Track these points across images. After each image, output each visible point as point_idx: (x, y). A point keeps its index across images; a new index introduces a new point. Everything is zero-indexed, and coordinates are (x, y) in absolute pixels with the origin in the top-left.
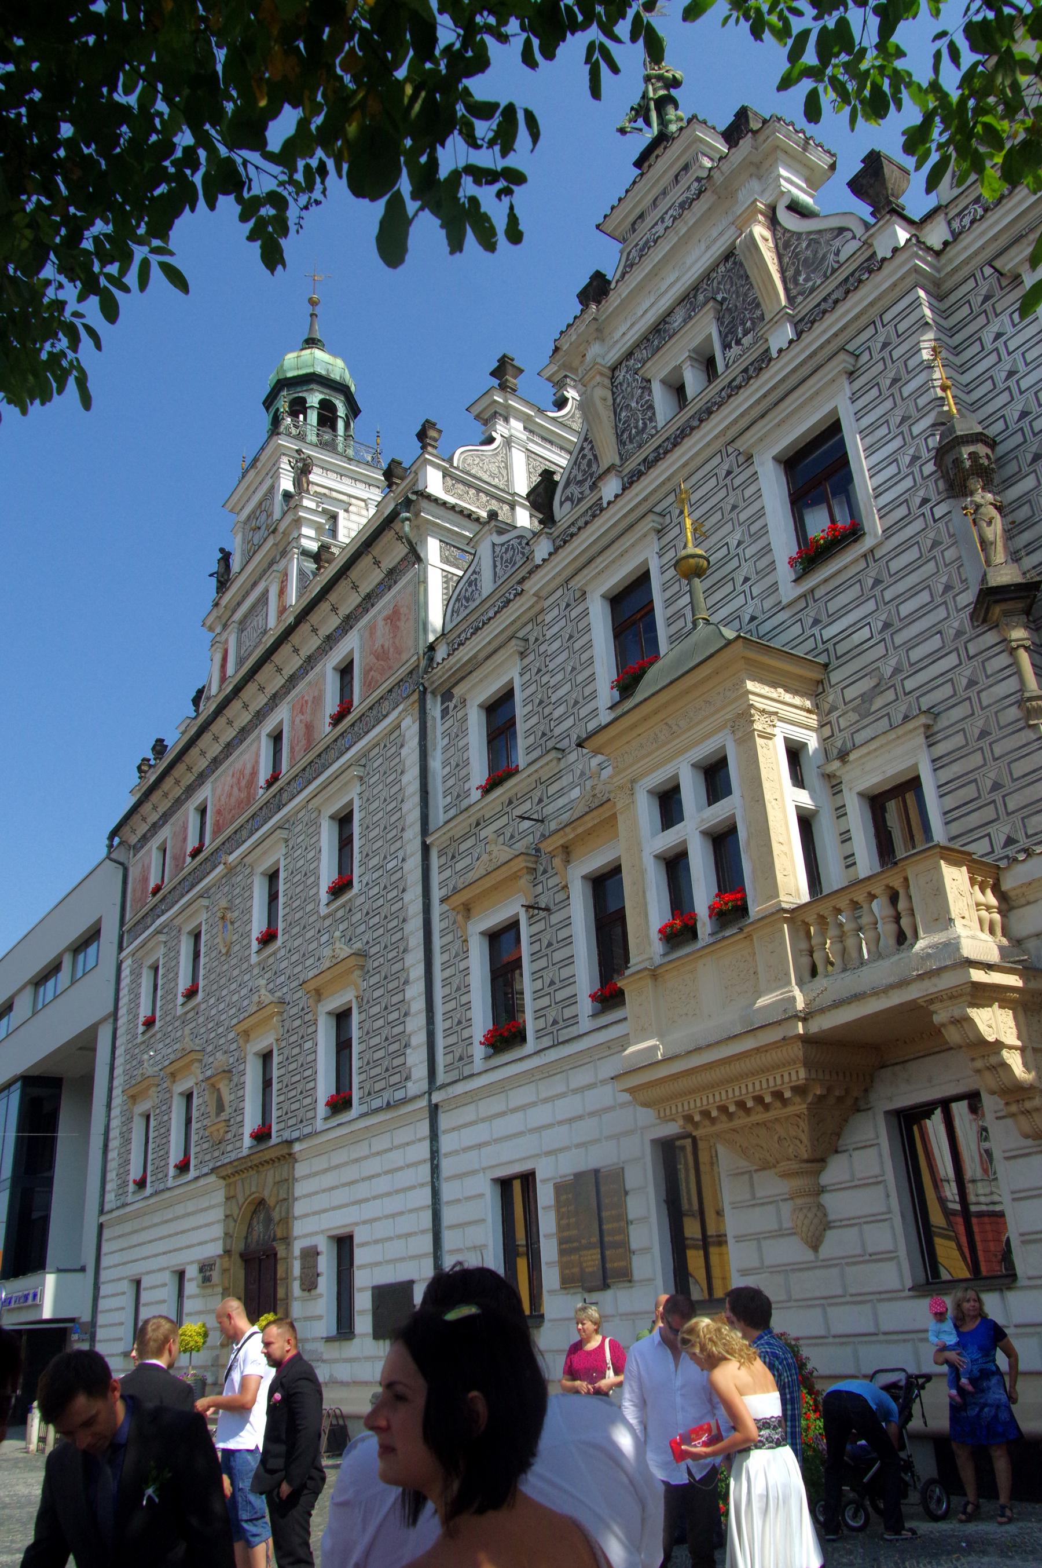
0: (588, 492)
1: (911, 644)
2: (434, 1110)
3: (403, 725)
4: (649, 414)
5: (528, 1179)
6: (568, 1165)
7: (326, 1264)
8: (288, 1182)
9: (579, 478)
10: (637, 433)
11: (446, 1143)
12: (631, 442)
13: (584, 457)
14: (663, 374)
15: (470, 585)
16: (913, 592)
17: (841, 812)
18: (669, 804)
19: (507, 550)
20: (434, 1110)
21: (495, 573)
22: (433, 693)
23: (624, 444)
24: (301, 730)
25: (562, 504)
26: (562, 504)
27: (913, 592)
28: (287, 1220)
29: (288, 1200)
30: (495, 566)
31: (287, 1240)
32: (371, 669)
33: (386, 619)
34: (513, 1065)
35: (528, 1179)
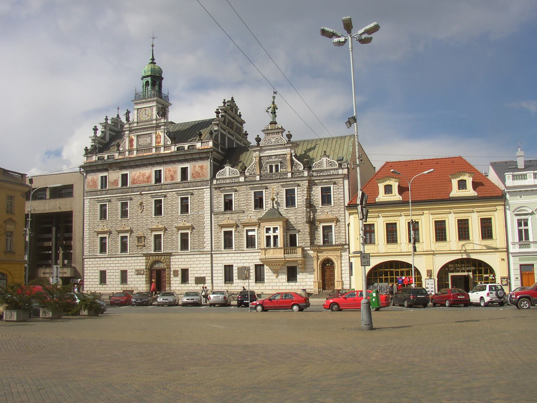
1: (298, 221)
2: (212, 254)
5: (231, 266)
6: (240, 265)
7: (180, 273)
8: (170, 259)
11: (214, 259)
16: (300, 216)
17: (287, 235)
18: (268, 230)
20: (212, 254)
27: (300, 216)
28: (170, 265)
29: (170, 262)
31: (170, 268)
33: (199, 166)
34: (228, 251)
35: (231, 266)
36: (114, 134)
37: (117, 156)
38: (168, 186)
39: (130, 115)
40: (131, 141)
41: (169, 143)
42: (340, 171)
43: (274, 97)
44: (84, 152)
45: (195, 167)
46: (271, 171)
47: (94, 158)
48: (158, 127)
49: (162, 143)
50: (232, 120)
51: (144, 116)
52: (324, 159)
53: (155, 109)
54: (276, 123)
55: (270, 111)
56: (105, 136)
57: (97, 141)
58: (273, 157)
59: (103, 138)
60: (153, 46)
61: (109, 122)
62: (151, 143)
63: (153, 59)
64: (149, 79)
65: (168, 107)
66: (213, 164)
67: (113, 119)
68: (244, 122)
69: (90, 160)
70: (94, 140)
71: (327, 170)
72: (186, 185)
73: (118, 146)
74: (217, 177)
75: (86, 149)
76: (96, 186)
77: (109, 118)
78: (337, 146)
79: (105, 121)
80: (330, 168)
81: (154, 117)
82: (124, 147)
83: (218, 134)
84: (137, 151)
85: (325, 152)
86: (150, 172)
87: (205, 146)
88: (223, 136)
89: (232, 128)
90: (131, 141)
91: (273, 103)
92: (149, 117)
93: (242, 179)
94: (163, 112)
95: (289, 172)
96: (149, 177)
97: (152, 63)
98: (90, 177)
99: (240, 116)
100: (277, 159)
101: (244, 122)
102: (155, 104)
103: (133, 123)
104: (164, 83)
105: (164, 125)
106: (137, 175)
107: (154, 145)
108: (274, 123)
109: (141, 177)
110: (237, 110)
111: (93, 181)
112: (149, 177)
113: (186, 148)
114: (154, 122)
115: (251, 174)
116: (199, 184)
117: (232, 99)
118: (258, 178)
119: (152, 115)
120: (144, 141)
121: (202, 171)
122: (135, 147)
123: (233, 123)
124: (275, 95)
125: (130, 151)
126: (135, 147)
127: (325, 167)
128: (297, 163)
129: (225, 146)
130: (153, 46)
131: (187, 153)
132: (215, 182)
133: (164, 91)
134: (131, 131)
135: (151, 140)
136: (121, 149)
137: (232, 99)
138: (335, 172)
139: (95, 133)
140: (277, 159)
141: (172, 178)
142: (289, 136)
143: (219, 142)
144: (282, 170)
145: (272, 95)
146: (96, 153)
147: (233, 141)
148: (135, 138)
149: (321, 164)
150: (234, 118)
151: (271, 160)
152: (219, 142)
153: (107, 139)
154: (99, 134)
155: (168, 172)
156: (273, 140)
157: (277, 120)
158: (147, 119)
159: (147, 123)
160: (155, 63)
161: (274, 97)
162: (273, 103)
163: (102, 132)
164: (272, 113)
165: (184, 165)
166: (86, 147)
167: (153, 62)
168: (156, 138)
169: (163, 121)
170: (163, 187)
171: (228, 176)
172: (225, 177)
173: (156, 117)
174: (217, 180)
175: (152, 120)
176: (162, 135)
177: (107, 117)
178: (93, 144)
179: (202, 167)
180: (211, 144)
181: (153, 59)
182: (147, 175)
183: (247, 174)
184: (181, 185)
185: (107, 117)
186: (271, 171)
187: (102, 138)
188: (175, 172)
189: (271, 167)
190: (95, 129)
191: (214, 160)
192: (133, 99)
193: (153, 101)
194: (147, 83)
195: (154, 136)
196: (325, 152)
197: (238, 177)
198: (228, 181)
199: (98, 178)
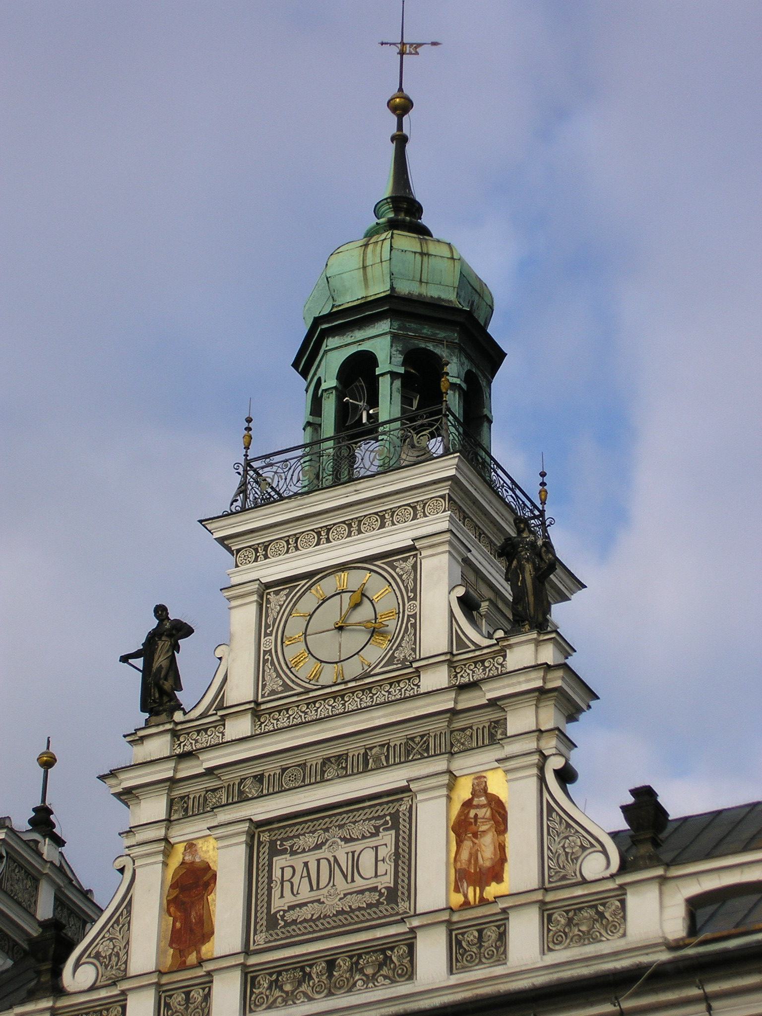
39: (188, 655)
40: (191, 888)
49: (522, 871)
51: (327, 645)
60: (401, 107)
62: (400, 891)
64: (379, 342)
81: (434, 637)
90: (191, 888)
92: (375, 653)
104: (504, 390)
119: (412, 624)
130: (401, 107)
135: (404, 858)
148: (229, 862)
158: (353, 669)
168: (462, 828)
169: (522, 654)
173: (457, 640)
194: (360, 369)
195: (432, 820)
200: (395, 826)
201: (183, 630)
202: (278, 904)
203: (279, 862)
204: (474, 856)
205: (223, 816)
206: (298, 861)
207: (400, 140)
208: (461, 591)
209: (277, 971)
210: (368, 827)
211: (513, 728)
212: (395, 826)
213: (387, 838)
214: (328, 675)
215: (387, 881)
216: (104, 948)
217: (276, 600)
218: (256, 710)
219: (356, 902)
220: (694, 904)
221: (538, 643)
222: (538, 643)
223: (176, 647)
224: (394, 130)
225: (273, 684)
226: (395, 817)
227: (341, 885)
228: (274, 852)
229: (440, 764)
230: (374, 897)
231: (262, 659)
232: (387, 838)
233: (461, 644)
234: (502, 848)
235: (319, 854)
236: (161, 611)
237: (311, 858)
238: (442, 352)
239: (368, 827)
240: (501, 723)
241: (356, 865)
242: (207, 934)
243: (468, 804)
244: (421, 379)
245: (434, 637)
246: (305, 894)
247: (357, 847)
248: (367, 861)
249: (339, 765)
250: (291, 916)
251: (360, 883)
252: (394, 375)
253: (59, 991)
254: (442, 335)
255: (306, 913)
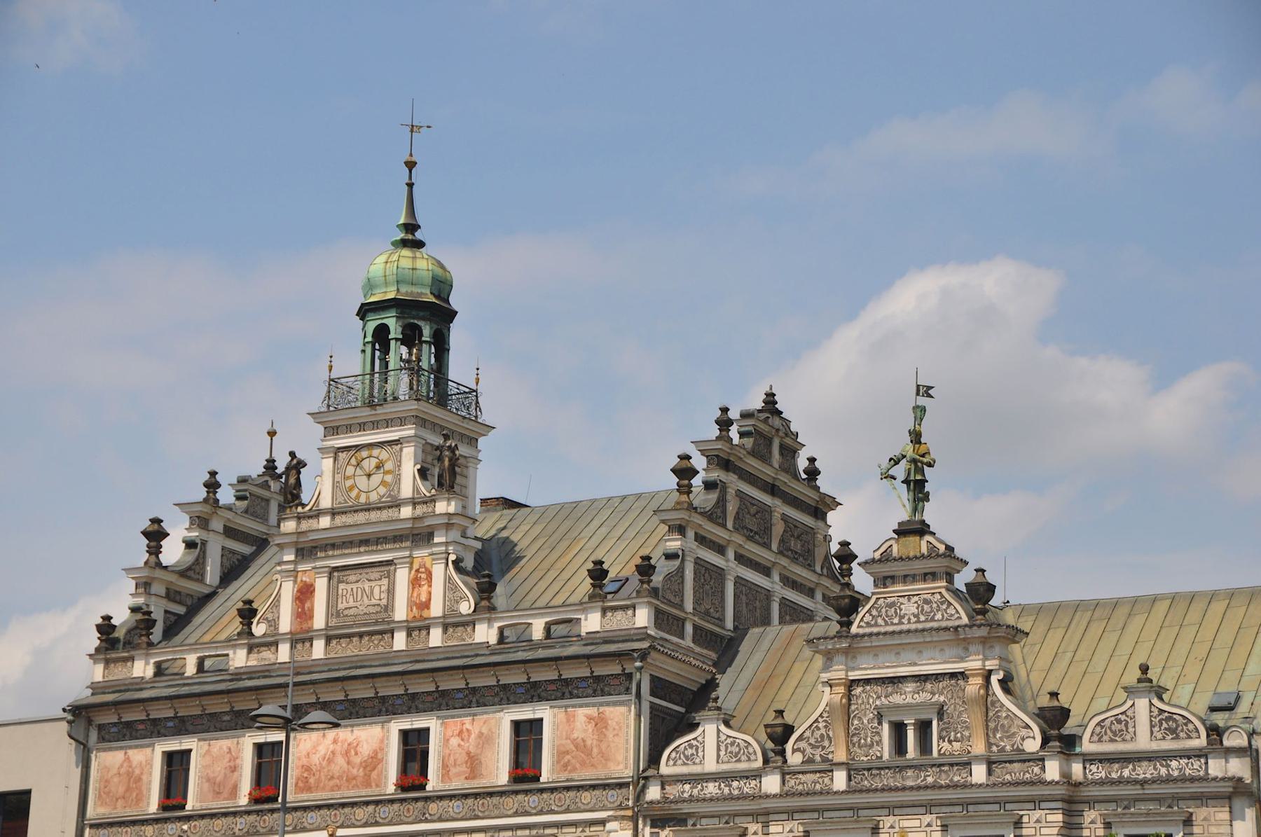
0: (818, 758)
3: (609, 826)
4: (877, 738)
9: (812, 741)
10: (866, 745)
12: (860, 747)
13: (818, 728)
14: (893, 719)
15: (691, 746)
19: (732, 744)
21: (718, 756)
22: (645, 817)
23: (854, 745)
24: (462, 757)
25: (794, 751)
26: (794, 751)
30: (719, 749)
32: (567, 753)
33: (590, 718)
36: (246, 549)
37: (239, 659)
38: (455, 806)
40: (305, 593)
41: (466, 608)
42: (1216, 767)
43: (920, 412)
44: (93, 640)
45: (570, 720)
46: (900, 746)
47: (142, 668)
48: (420, 536)
49: (436, 610)
50: (766, 499)
52: (1142, 704)
53: (409, 452)
54: (922, 529)
55: (900, 471)
56: (200, 562)
57: (158, 588)
58: (910, 687)
59: (192, 571)
60: (411, 165)
61: (226, 496)
62: (389, 608)
63: (411, 227)
65: (473, 442)
66: (653, 707)
67: (243, 480)
68: (833, 504)
69: (118, 673)
70: (144, 585)
71: (1150, 757)
72: (533, 800)
73: (248, 613)
74: (665, 769)
75: (106, 627)
76: (139, 799)
77: (227, 479)
78: (1226, 636)
79: (202, 493)
80: (1168, 745)
82: (273, 623)
83: (681, 570)
84: (329, 640)
85: (1144, 669)
86: (380, 739)
87: (619, 621)
88: (709, 577)
89: (761, 535)
90: (305, 593)
91: (916, 437)
93: (771, 783)
94: (446, 470)
95: (978, 759)
96: (374, 762)
97: (404, 243)
98: (108, 760)
99: (813, 473)
100: (923, 697)
101: (833, 504)
102: (409, 431)
103: (317, 514)
104: (457, 334)
105: (448, 526)
106: (322, 750)
107: (401, 612)
108: (914, 529)
109: (340, 761)
110: (790, 451)
111: (129, 774)
112: (374, 762)
113: (538, 633)
114: (406, 512)
115: (810, 761)
116: (586, 797)
117: (770, 399)
118: (840, 780)
120: (361, 596)
121: (602, 736)
122: (319, 622)
123: (765, 511)
124: (922, 401)
125: (301, 639)
126: (319, 622)
127: (1143, 741)
128: (1011, 717)
129: (722, 620)
130: (411, 165)
131: (541, 653)
132: (653, 793)
133: (459, 371)
134: (306, 551)
135: (391, 592)
136: (259, 629)
137: (770, 399)
138: (1193, 767)
139: (155, 550)
140: (923, 697)
141: (474, 764)
142: (981, 592)
143: (689, 606)
144: (945, 745)
145: (910, 399)
146: (150, 645)
147: (768, 594)
148: (321, 585)
149: (1123, 726)
150: (772, 490)
151: (897, 699)
152: (689, 606)
153: (212, 574)
154: (173, 552)
155: (454, 741)
156: (909, 608)
157: (931, 514)
158: (374, 497)
159: (374, 516)
160: (419, 244)
161: (920, 412)
162: (916, 437)
163: (190, 545)
164: (906, 481)
165: (525, 712)
166: (107, 618)
167: (411, 239)
168: (415, 583)
170: (433, 807)
171: (710, 766)
172: (696, 769)
174: (664, 782)
175: (397, 504)
176: (438, 571)
177: (213, 474)
178: (140, 600)
179: (600, 724)
180: (643, 617)
181: (411, 227)
182: (366, 750)
183: (794, 759)
184: (511, 803)
185: (213, 474)
186: (900, 746)
187: (184, 573)
188: (486, 740)
189: (899, 730)
190: (155, 535)
191: (660, 687)
192: (317, 405)
193: (402, 421)
194: (381, 334)
195: (402, 576)
196: (1144, 669)
197: (757, 775)
198: (711, 789)
199: (150, 763)
200: (388, 577)
201: (302, 464)
202: (340, 606)
203: (342, 586)
204: (419, 595)
205: (319, 564)
206: (349, 587)
207: (410, 185)
208: (419, 467)
209: (340, 637)
210: (377, 575)
211: (436, 540)
212: (388, 577)
213: (385, 581)
214: (363, 499)
215: (384, 602)
216: (270, 616)
217: (342, 456)
218: (333, 513)
219: (372, 610)
220: (501, 630)
221: (449, 500)
222: (449, 500)
223: (299, 473)
224: (407, 180)
225: (341, 499)
226: (389, 572)
227: (366, 601)
228: (340, 582)
229: (407, 553)
230: (379, 609)
231: (335, 485)
232: (385, 581)
233: (418, 493)
234: (430, 593)
235: (359, 585)
236: (292, 454)
237: (354, 586)
238: (420, 323)
239: (377, 575)
240: (430, 536)
241: (372, 592)
242: (311, 617)
243: (417, 571)
244: (410, 337)
245: (406, 491)
246: (351, 604)
247: (373, 584)
248: (376, 590)
249: (365, 542)
250: (346, 612)
251: (374, 602)
252: (397, 339)
253: (251, 634)
254: (421, 314)
255: (352, 612)
